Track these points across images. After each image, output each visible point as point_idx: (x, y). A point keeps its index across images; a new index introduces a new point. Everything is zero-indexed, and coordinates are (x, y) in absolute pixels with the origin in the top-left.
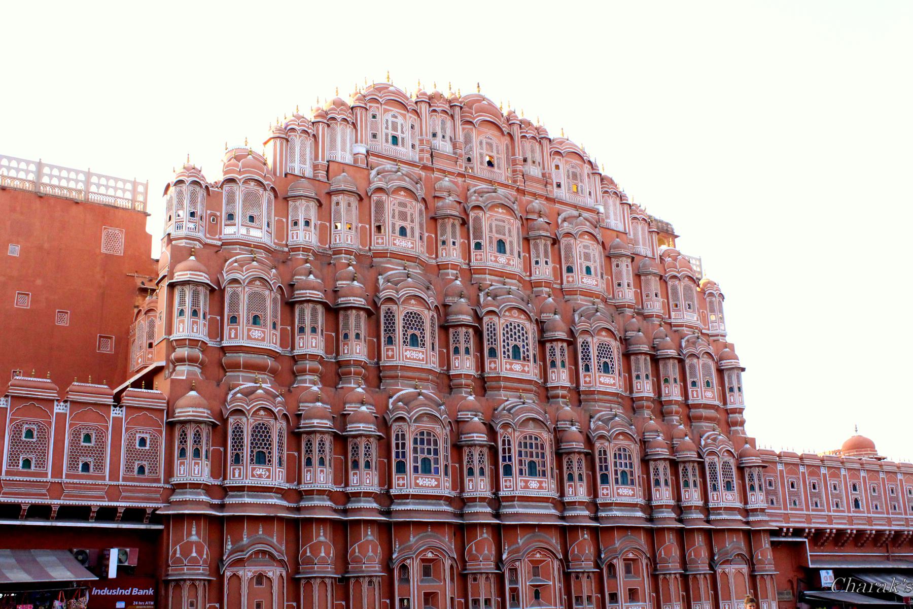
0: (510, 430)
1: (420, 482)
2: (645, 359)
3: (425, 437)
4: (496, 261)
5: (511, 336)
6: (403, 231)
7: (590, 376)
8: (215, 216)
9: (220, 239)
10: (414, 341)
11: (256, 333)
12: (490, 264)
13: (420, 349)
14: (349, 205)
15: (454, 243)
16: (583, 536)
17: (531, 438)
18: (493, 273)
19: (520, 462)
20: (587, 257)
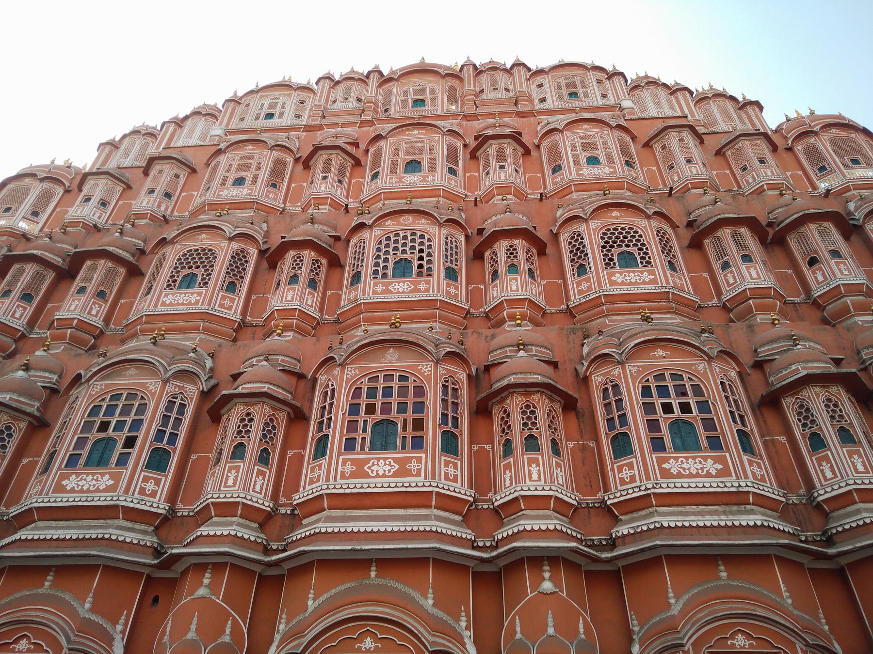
0: (337, 371)
1: (71, 483)
2: (736, 236)
4: (401, 181)
6: (239, 182)
7: (588, 280)
10: (189, 281)
13: (196, 290)
14: (160, 172)
16: (536, 585)
17: (389, 378)
19: (352, 426)
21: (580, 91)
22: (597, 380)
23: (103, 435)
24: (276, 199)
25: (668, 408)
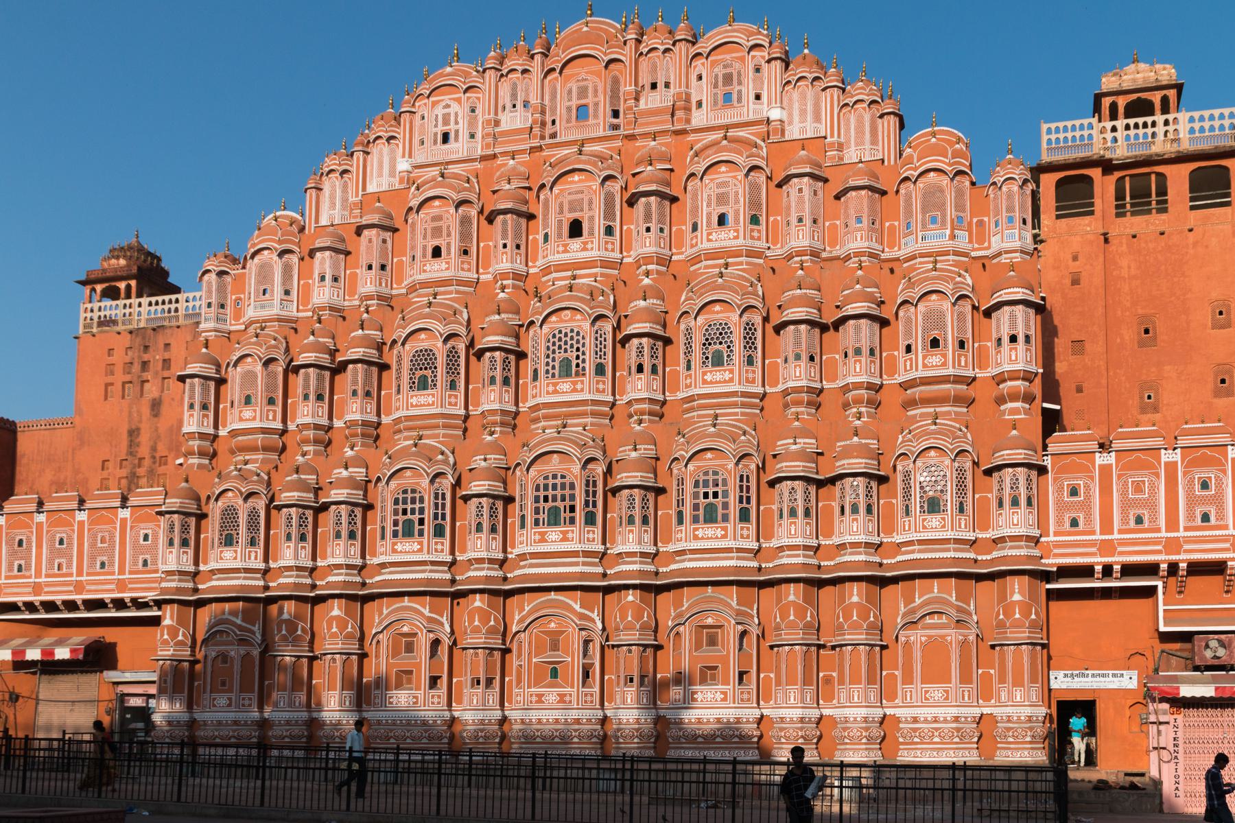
1: (399, 547)
3: (409, 496)
4: (565, 251)
5: (560, 347)
6: (437, 252)
8: (240, 299)
10: (423, 384)
11: (247, 413)
13: (429, 391)
15: (505, 246)
17: (555, 477)
18: (561, 267)
19: (537, 511)
22: (675, 471)
23: (405, 517)
24: (469, 270)
25: (706, 495)
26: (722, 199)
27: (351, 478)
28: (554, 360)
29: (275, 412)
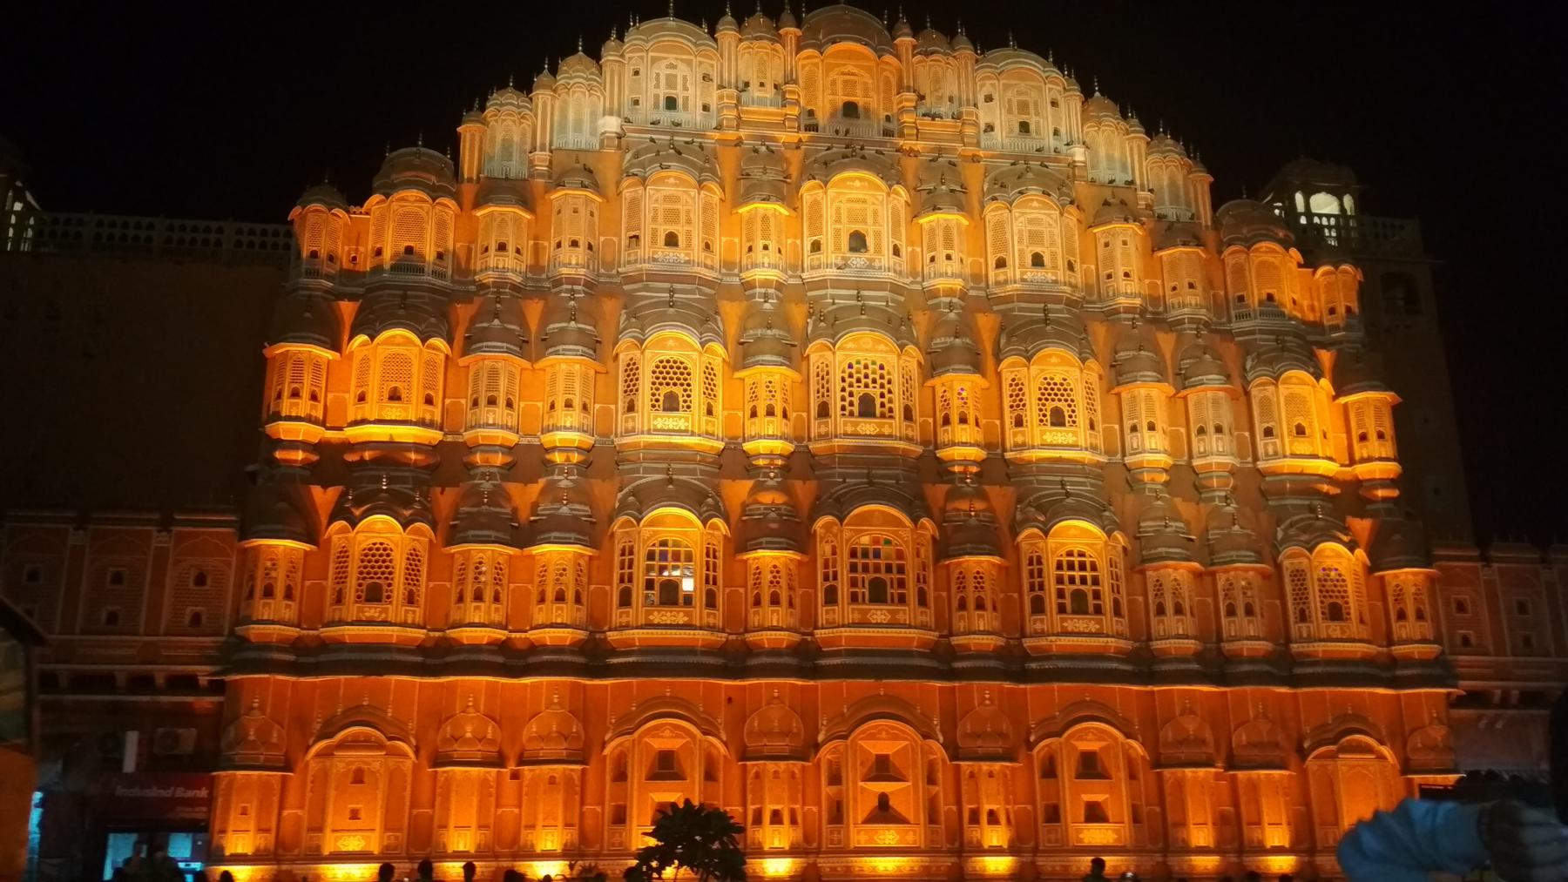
3: (670, 549)
6: (671, 240)
7: (1023, 434)
9: (362, 285)
10: (671, 404)
11: (394, 411)
12: (831, 273)
15: (766, 248)
18: (838, 284)
19: (854, 583)
20: (1035, 237)
21: (1033, 121)
26: (1035, 237)
27: (576, 518)
28: (851, 394)
29: (432, 413)
